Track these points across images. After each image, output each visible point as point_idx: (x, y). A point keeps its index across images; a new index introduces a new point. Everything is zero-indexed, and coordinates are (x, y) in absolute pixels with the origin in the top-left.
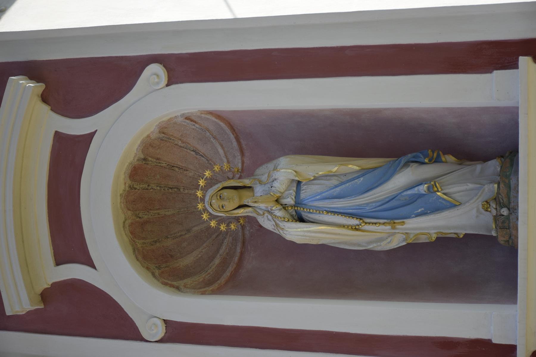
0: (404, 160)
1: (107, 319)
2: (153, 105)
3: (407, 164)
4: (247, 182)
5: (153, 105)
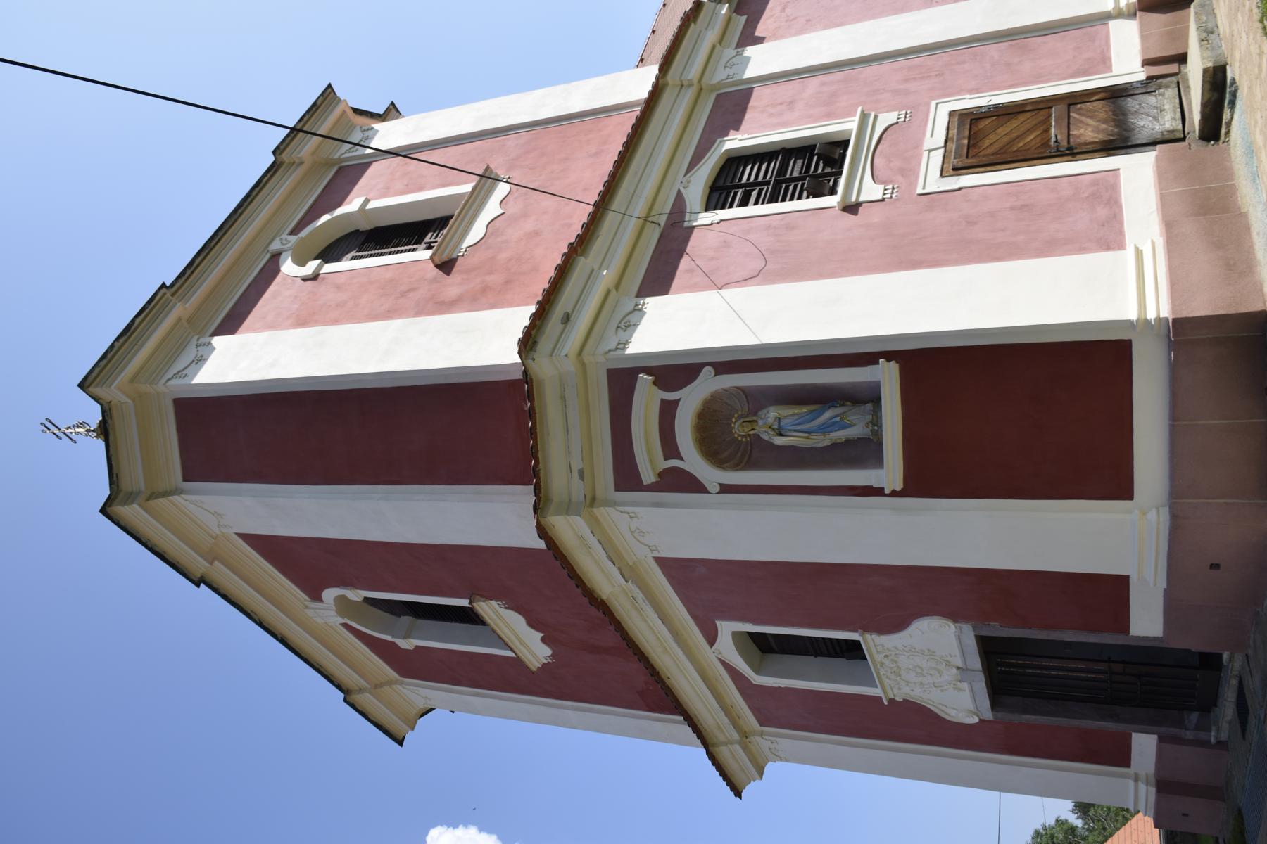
1: (691, 484)
2: (706, 385)
5: (706, 385)
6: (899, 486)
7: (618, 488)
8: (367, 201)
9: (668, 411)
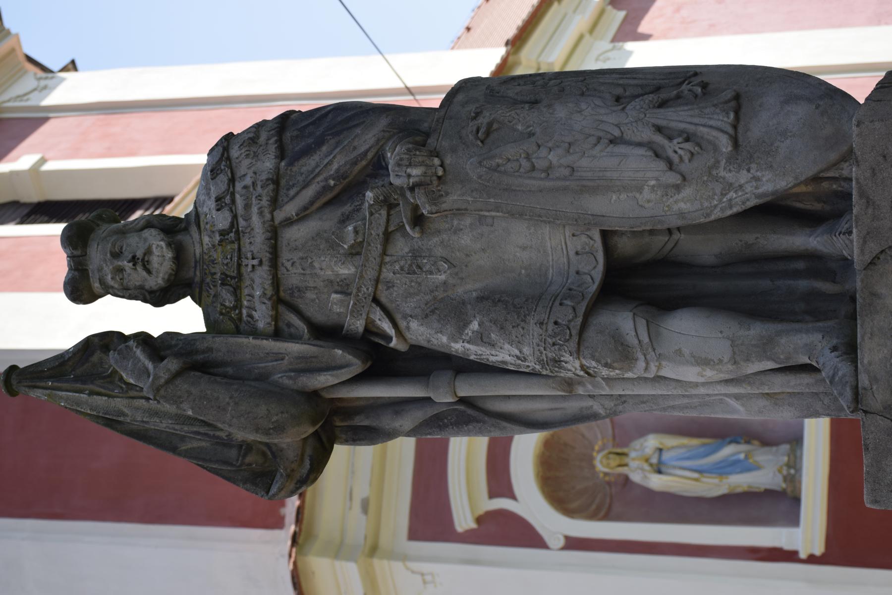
0: (728, 440)
3: (730, 442)
4: (625, 450)
6: (819, 549)
7: (413, 535)
8: (43, 161)
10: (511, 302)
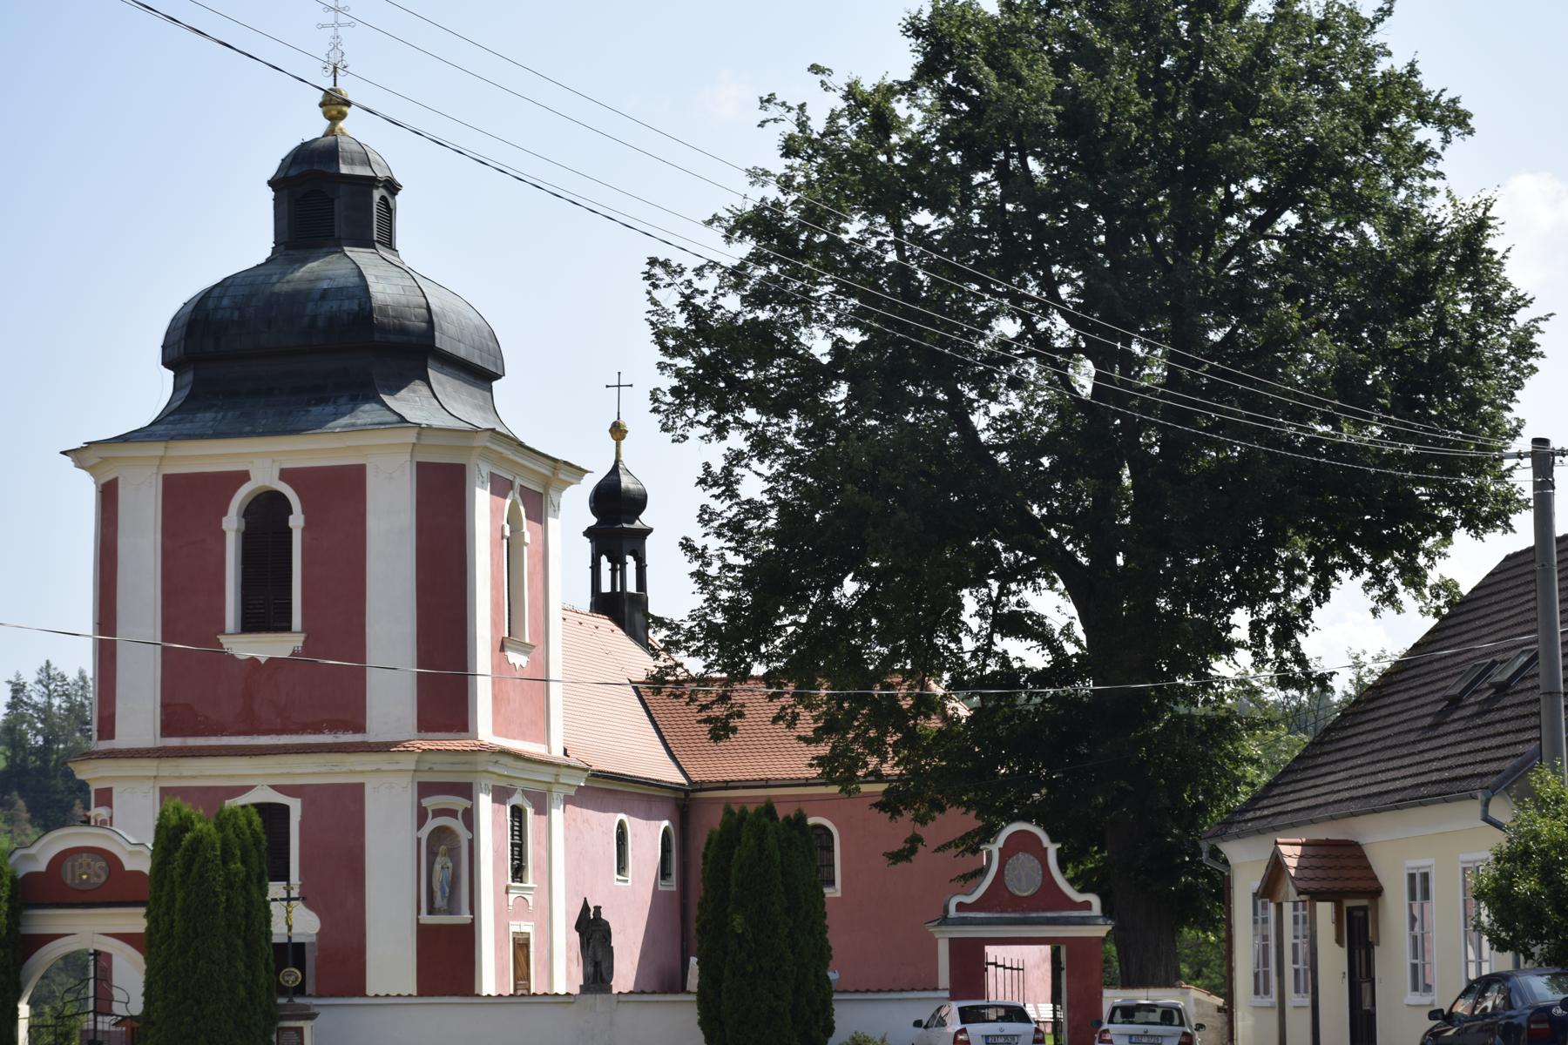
5: (464, 834)
7: (419, 784)
9: (452, 813)
10: (595, 953)
